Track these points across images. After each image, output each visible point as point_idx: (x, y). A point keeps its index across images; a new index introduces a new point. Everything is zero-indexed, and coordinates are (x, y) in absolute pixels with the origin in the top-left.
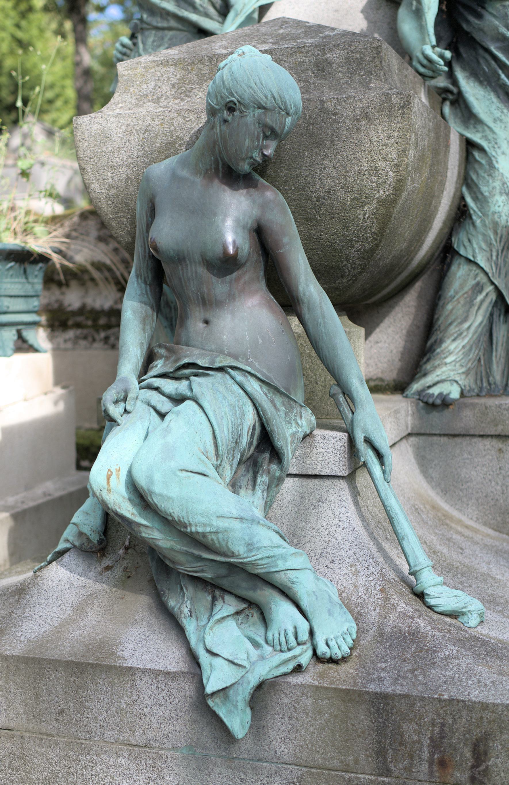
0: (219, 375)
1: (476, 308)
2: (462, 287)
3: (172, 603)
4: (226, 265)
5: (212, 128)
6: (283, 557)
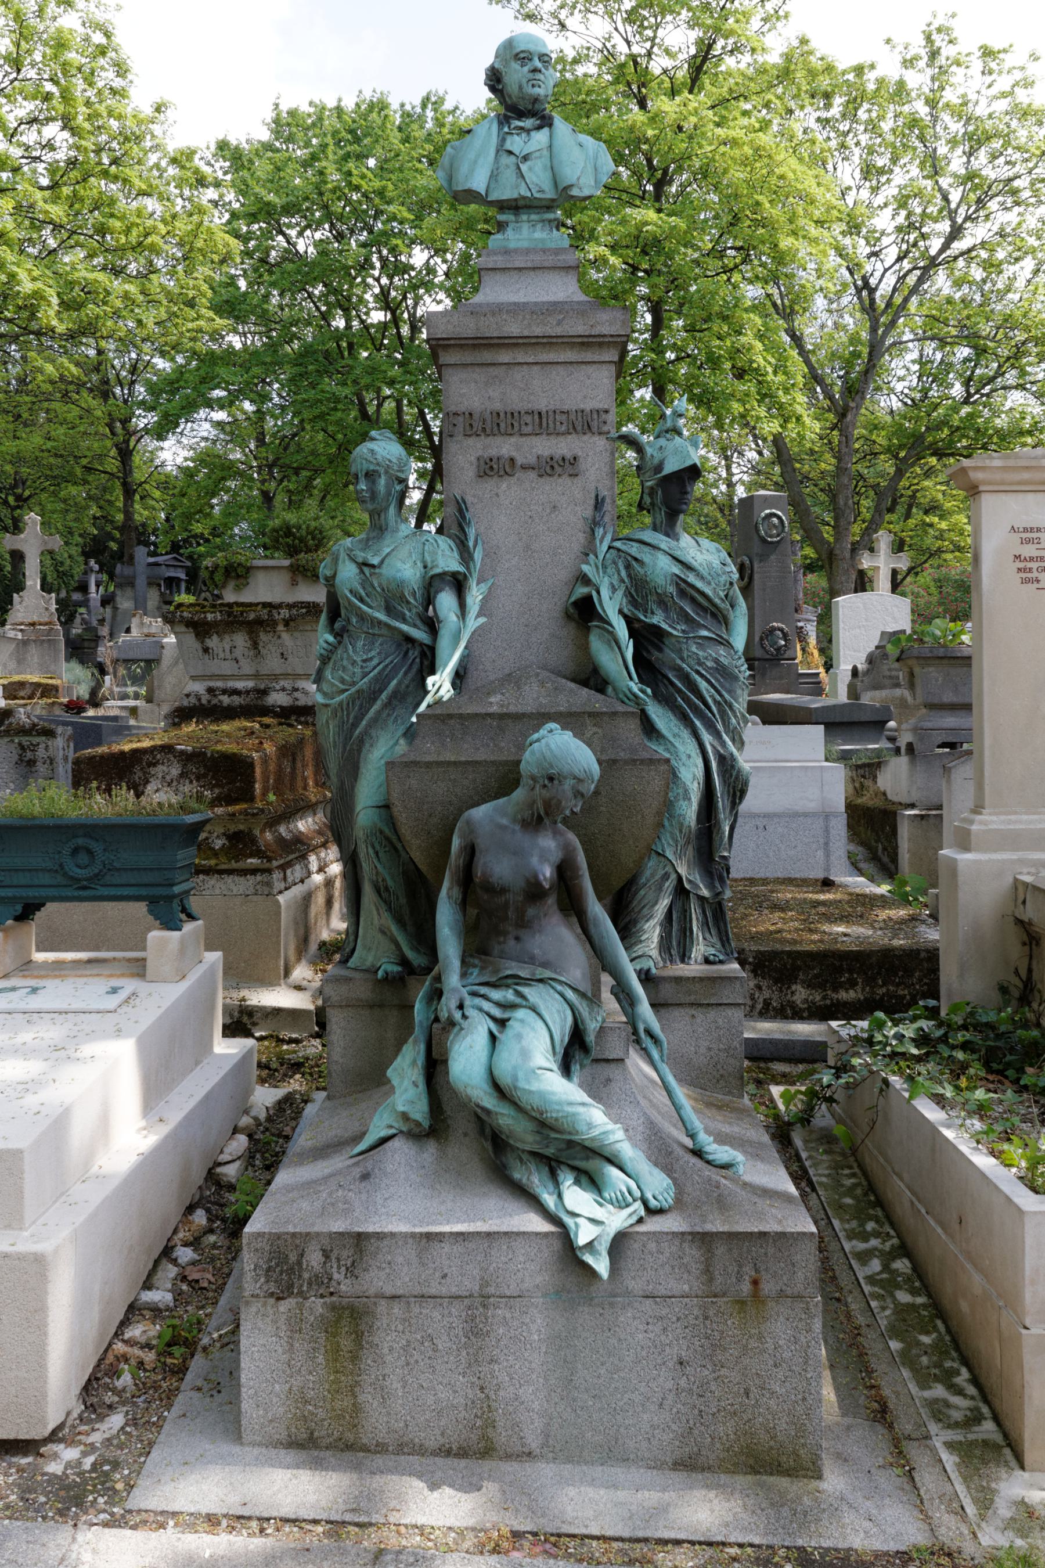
0: (541, 985)
2: (652, 875)
3: (517, 1176)
4: (534, 892)
5: (533, 789)
6: (613, 1132)
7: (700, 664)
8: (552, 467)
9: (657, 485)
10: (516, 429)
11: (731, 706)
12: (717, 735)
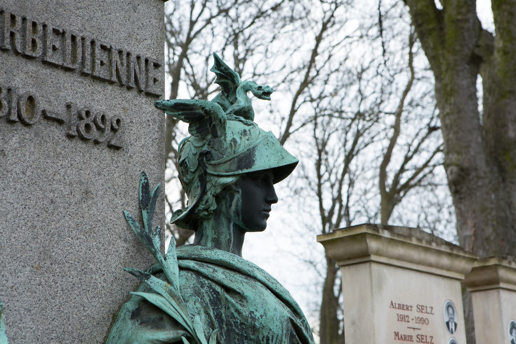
8: (88, 127)
9: (236, 184)
10: (38, 53)
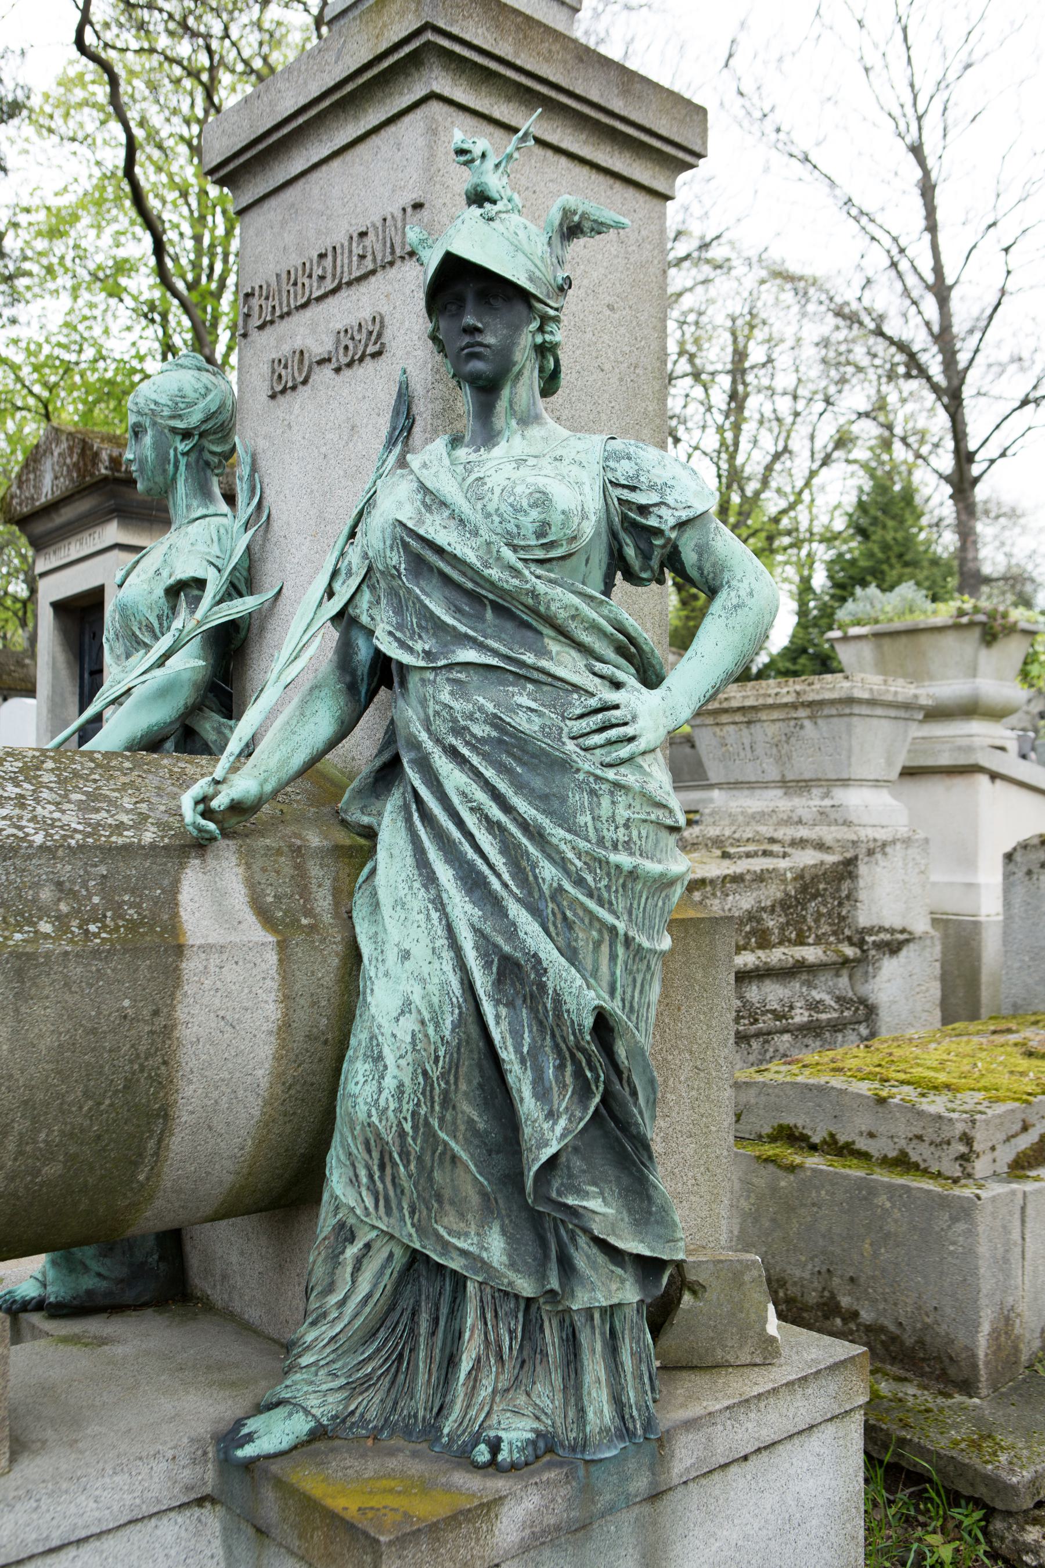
1: (349, 1269)
7: (459, 731)
11: (538, 836)
12: (493, 904)
